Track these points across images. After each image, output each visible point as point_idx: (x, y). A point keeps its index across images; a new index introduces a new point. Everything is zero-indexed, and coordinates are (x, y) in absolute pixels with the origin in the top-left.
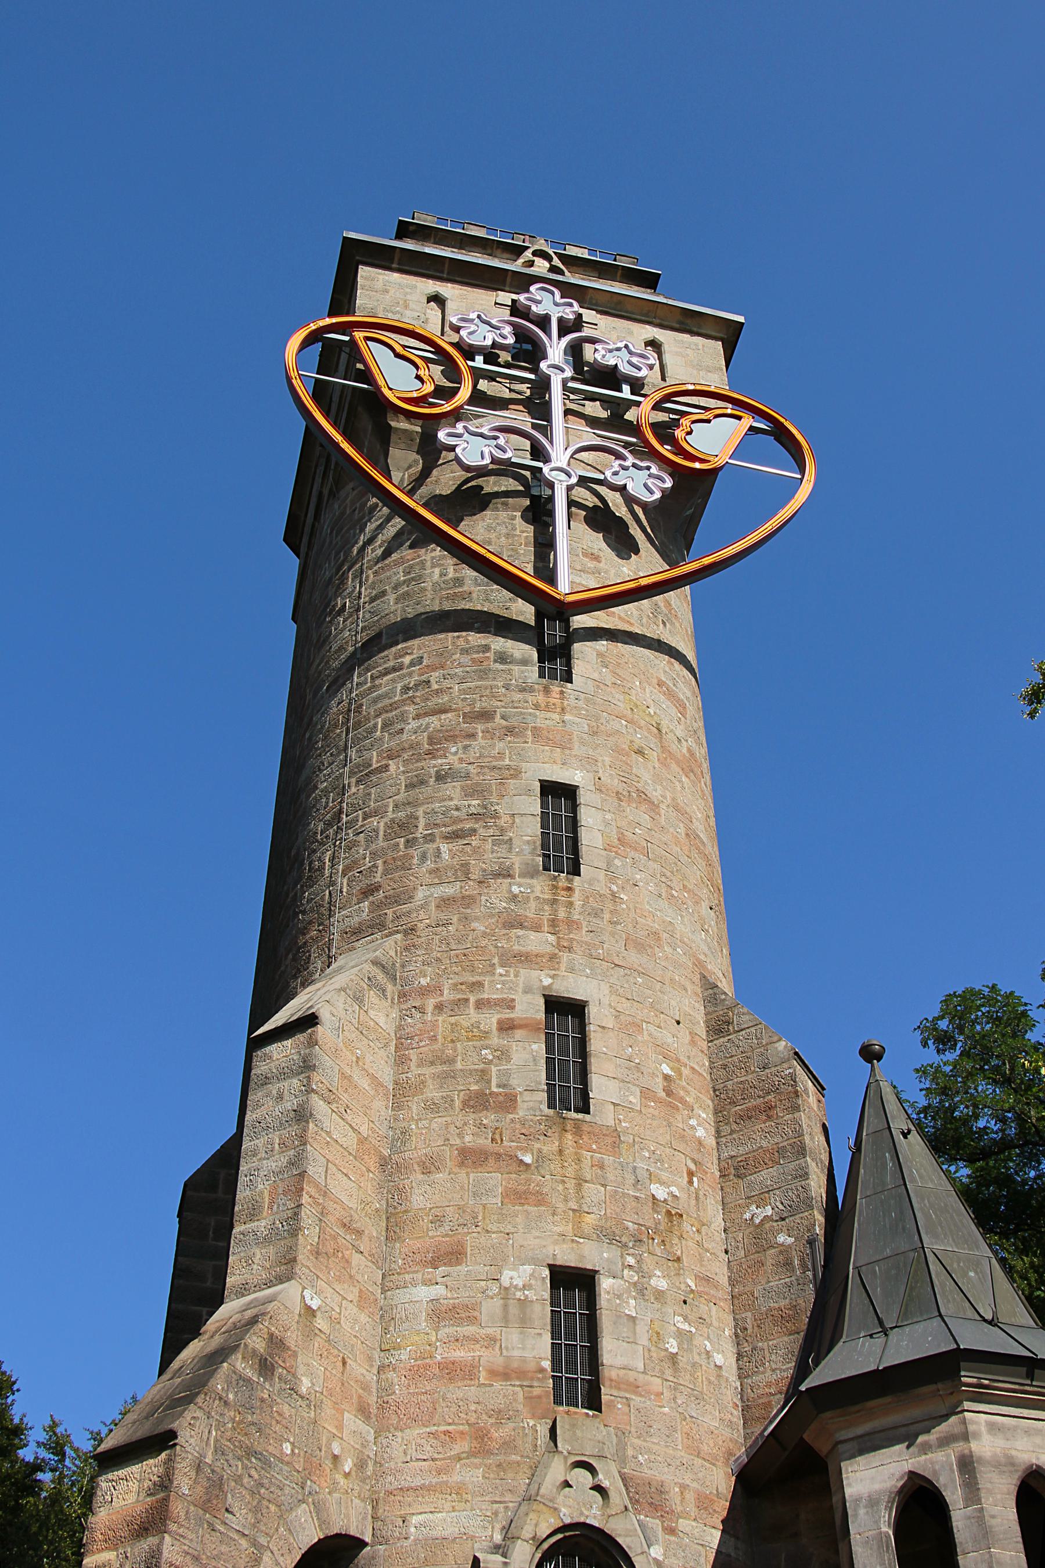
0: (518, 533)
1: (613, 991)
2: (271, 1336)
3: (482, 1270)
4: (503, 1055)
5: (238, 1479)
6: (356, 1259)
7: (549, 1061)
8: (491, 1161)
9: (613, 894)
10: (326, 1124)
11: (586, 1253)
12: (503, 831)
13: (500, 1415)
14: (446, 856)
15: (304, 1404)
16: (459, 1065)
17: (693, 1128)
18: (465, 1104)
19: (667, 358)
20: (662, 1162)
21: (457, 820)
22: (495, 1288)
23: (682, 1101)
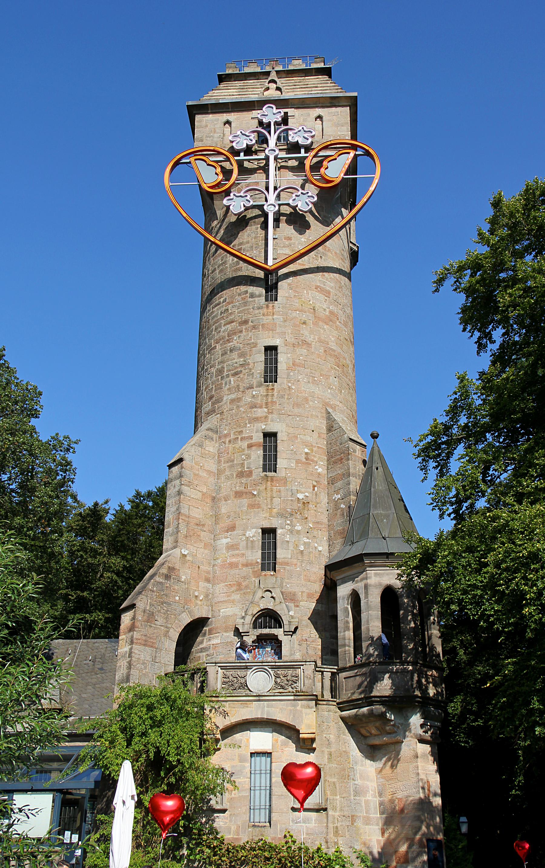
0: (259, 235)
1: (287, 425)
2: (169, 567)
3: (241, 532)
4: (249, 457)
6: (202, 534)
7: (265, 456)
8: (244, 495)
9: (289, 387)
10: (188, 494)
11: (273, 522)
12: (250, 369)
14: (232, 383)
15: (183, 584)
16: (235, 462)
17: (317, 469)
18: (237, 476)
19: (324, 123)
20: (302, 485)
21: (236, 368)
23: (312, 461)
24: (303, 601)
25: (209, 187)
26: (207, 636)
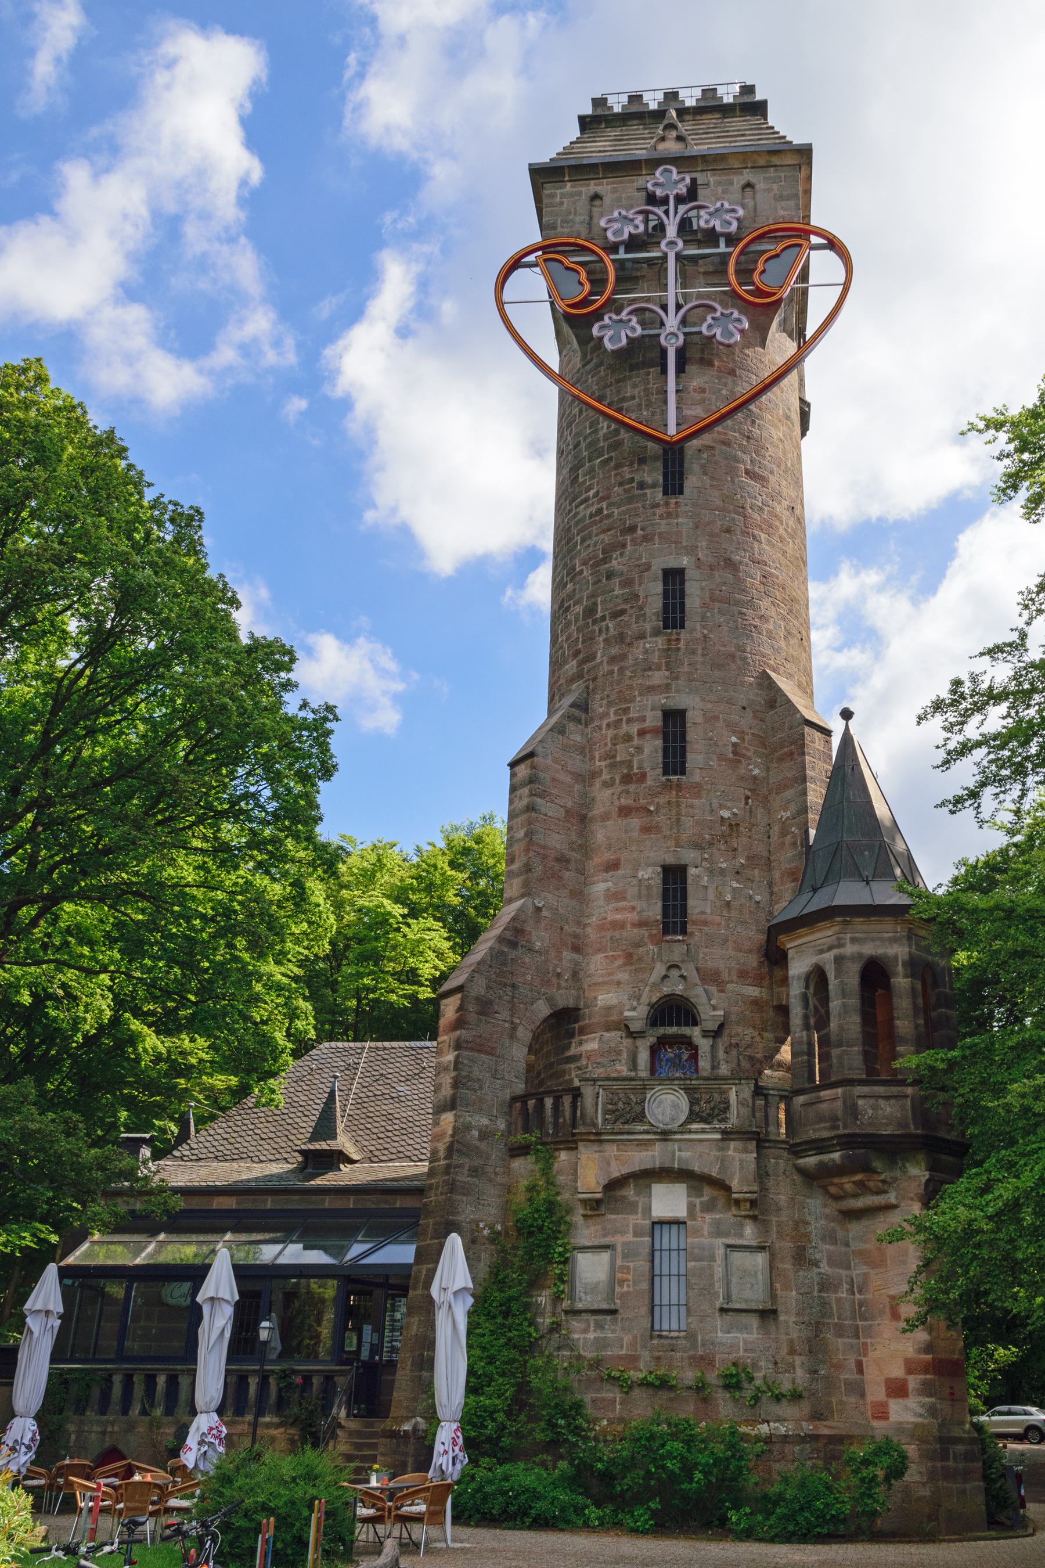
1: (703, 700)
3: (629, 872)
4: (639, 749)
5: (500, 998)
6: (567, 875)
7: (666, 750)
9: (705, 636)
10: (543, 810)
12: (641, 608)
13: (638, 945)
16: (618, 759)
18: (621, 782)
22: (635, 882)
23: (743, 756)
24: (732, 982)
25: (569, 306)
26: (577, 1039)
